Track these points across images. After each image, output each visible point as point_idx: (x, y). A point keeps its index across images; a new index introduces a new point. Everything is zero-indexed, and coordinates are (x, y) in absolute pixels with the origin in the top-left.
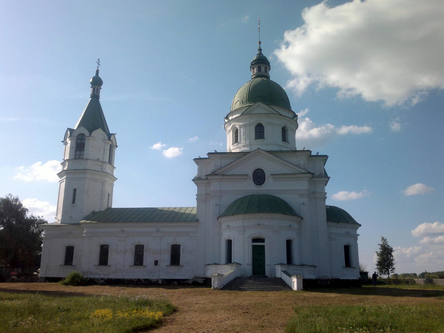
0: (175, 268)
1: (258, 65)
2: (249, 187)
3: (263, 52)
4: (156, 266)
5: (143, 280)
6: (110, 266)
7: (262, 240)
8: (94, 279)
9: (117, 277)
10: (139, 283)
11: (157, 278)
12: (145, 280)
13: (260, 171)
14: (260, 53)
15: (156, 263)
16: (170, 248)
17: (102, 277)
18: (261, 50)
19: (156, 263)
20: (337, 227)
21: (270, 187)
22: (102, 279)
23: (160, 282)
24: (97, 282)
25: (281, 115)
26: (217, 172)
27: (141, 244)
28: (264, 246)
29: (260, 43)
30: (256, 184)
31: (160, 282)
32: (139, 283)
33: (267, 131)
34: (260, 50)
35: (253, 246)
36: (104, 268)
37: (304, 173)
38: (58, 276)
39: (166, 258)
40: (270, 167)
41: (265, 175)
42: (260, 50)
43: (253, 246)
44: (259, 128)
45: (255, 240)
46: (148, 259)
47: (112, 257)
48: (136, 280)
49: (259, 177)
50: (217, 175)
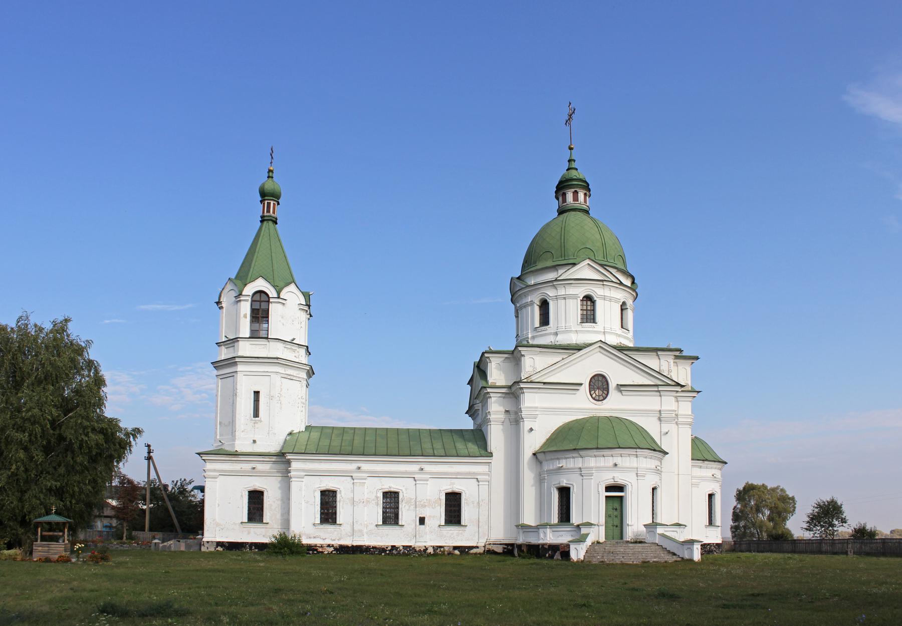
0: (453, 530)
2: (581, 405)
7: (620, 488)
8: (316, 546)
10: (394, 552)
11: (428, 544)
13: (600, 378)
15: (422, 521)
16: (443, 498)
19: (422, 521)
20: (701, 467)
21: (615, 405)
22: (329, 546)
23: (430, 550)
24: (320, 550)
25: (621, 283)
26: (533, 378)
27: (392, 490)
30: (594, 399)
31: (430, 550)
36: (329, 528)
37: (669, 385)
39: (438, 513)
40: (618, 373)
44: (585, 303)
45: (608, 489)
46: (406, 514)
47: (343, 511)
49: (599, 385)
50: (531, 382)
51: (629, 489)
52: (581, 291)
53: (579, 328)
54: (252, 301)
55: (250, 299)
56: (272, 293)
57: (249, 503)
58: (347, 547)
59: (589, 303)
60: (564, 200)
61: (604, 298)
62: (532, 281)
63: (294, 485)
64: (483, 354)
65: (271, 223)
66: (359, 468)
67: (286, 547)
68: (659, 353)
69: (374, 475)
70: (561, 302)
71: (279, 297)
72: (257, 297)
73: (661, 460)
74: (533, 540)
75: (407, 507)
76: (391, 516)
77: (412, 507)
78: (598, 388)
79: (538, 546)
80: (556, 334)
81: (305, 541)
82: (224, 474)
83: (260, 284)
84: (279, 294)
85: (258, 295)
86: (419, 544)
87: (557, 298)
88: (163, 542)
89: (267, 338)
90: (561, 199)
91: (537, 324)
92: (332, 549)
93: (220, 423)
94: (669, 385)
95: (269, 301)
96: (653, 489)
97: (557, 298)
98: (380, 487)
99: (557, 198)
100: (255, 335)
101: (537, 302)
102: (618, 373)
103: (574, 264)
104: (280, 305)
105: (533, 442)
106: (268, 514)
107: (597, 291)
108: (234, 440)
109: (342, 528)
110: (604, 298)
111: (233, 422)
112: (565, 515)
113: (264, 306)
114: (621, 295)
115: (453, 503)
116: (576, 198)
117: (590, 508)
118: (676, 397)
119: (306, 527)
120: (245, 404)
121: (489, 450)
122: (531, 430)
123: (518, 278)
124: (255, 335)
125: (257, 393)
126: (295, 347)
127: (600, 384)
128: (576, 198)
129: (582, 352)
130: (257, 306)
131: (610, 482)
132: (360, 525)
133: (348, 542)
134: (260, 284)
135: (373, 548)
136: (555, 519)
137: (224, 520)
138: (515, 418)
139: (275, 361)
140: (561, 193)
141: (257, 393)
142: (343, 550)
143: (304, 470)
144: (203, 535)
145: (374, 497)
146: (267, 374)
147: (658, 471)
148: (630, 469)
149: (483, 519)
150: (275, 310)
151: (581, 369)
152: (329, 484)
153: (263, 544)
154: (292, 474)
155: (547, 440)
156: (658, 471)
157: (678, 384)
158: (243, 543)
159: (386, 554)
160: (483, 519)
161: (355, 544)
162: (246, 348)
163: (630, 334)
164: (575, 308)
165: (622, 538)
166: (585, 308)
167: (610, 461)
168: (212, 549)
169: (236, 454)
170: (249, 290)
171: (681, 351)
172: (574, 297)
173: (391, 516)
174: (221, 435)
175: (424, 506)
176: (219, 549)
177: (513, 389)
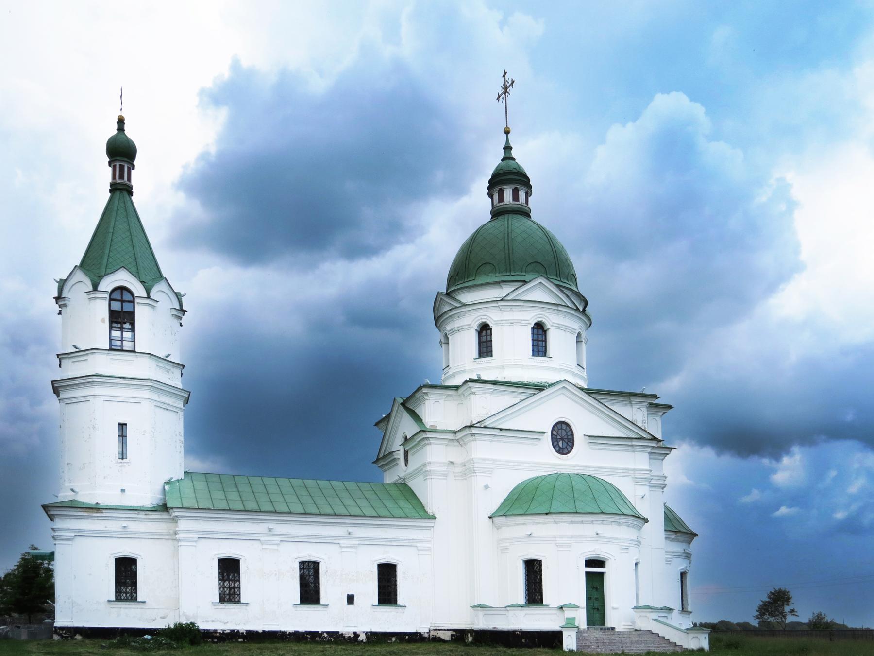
1: (513, 186)
2: (544, 460)
3: (514, 153)
7: (600, 563)
12: (330, 634)
13: (564, 427)
14: (508, 157)
18: (511, 148)
21: (582, 459)
28: (601, 575)
29: (507, 132)
33: (554, 339)
34: (508, 148)
35: (587, 573)
36: (230, 607)
37: (644, 439)
41: (573, 435)
42: (508, 148)
44: (535, 331)
45: (589, 563)
49: (563, 438)
52: (532, 316)
54: (111, 300)
55: (107, 296)
59: (540, 332)
60: (501, 199)
62: (466, 297)
64: (420, 388)
66: (270, 530)
68: (633, 399)
69: (288, 539)
71: (149, 297)
72: (117, 295)
73: (640, 528)
78: (562, 439)
80: (503, 367)
81: (202, 626)
83: (122, 278)
84: (148, 294)
85: (119, 292)
86: (347, 630)
87: (501, 323)
89: (134, 351)
90: (496, 197)
94: (644, 439)
95: (133, 302)
96: (636, 564)
97: (501, 323)
99: (491, 195)
101: (475, 326)
102: (585, 420)
103: (525, 282)
107: (551, 319)
110: (558, 327)
112: (534, 594)
113: (127, 307)
114: (576, 325)
116: (516, 197)
118: (650, 453)
121: (430, 512)
122: (487, 487)
123: (448, 294)
125: (122, 426)
126: (169, 366)
127: (564, 433)
128: (516, 197)
129: (543, 394)
130: (116, 306)
131: (592, 555)
134: (122, 278)
136: (521, 599)
137: (83, 597)
140: (497, 189)
141: (122, 426)
143: (197, 532)
147: (638, 543)
148: (607, 539)
150: (142, 314)
151: (543, 415)
154: (180, 535)
155: (505, 500)
156: (638, 543)
157: (655, 439)
163: (584, 374)
165: (603, 623)
166: (536, 338)
170: (108, 284)
171: (655, 397)
177: (459, 435)
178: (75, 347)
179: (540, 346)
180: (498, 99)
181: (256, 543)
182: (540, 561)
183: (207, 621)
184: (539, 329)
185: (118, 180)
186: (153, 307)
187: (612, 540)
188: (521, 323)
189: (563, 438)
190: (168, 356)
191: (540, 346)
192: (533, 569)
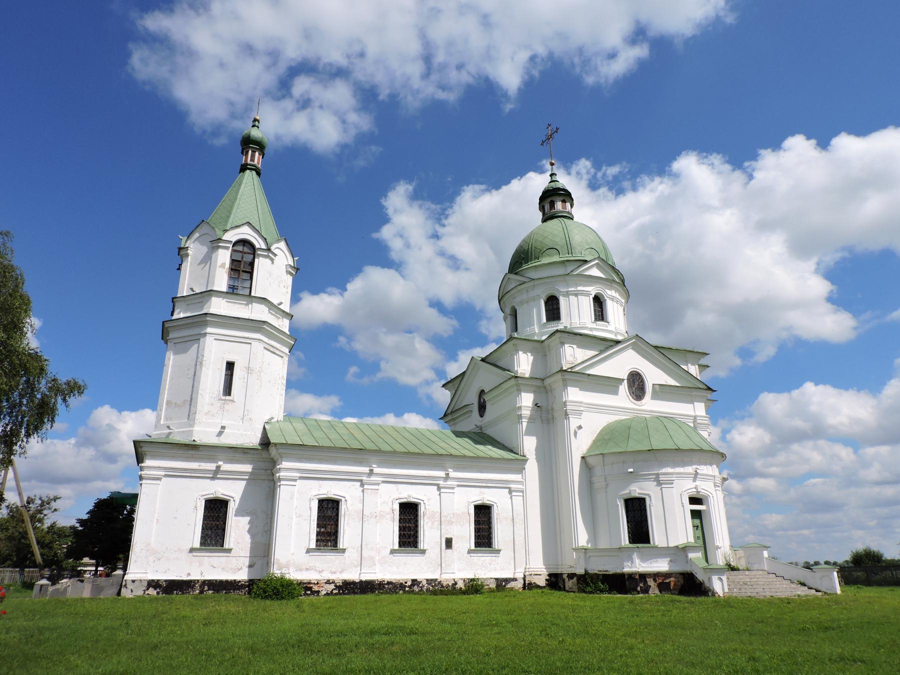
4: (449, 551)
5: (424, 582)
6: (344, 551)
8: (309, 583)
9: (365, 577)
10: (416, 588)
15: (449, 543)
17: (332, 577)
19: (449, 543)
22: (328, 582)
23: (461, 585)
24: (316, 588)
32: (416, 588)
38: (185, 578)
39: (465, 532)
43: (692, 512)
46: (429, 534)
48: (409, 583)
49: (636, 384)
51: (711, 501)
52: (593, 290)
53: (594, 326)
56: (259, 243)
57: (206, 518)
58: (354, 583)
61: (613, 299)
63: (284, 493)
65: (254, 172)
67: (268, 589)
68: (688, 355)
70: (572, 298)
74: (612, 568)
75: (430, 524)
76: (409, 536)
77: (437, 523)
79: (622, 576)
82: (173, 474)
87: (567, 294)
88: (53, 584)
91: (545, 321)
92: (332, 586)
93: (168, 403)
98: (396, 497)
100: (232, 292)
104: (268, 261)
105: (580, 444)
106: (233, 534)
108: (192, 426)
109: (347, 554)
110: (613, 299)
111: (192, 401)
115: (483, 513)
117: (671, 527)
119: (296, 557)
120: (212, 378)
124: (232, 292)
125: (230, 366)
132: (369, 552)
133: (354, 576)
135: (389, 583)
136: (625, 540)
137: (164, 546)
138: (549, 416)
139: (257, 326)
141: (230, 366)
142: (348, 588)
144: (125, 569)
145: (388, 510)
146: (247, 342)
149: (520, 540)
150: (261, 264)
152: (330, 490)
153: (221, 582)
158: (191, 581)
159: (405, 591)
160: (520, 540)
161: (364, 579)
162: (219, 306)
164: (587, 305)
167: (690, 469)
168: (140, 593)
169: (192, 449)
172: (587, 294)
173: (409, 536)
174: (166, 419)
175: (450, 523)
176: (152, 592)
178: (192, 289)
179: (600, 313)
180: (557, 129)
181: (359, 484)
182: (644, 499)
183: (301, 570)
184: (598, 301)
185: (249, 162)
186: (272, 260)
187: (707, 477)
188: (587, 294)
189: (636, 384)
190: (281, 303)
191: (600, 313)
192: (637, 510)
